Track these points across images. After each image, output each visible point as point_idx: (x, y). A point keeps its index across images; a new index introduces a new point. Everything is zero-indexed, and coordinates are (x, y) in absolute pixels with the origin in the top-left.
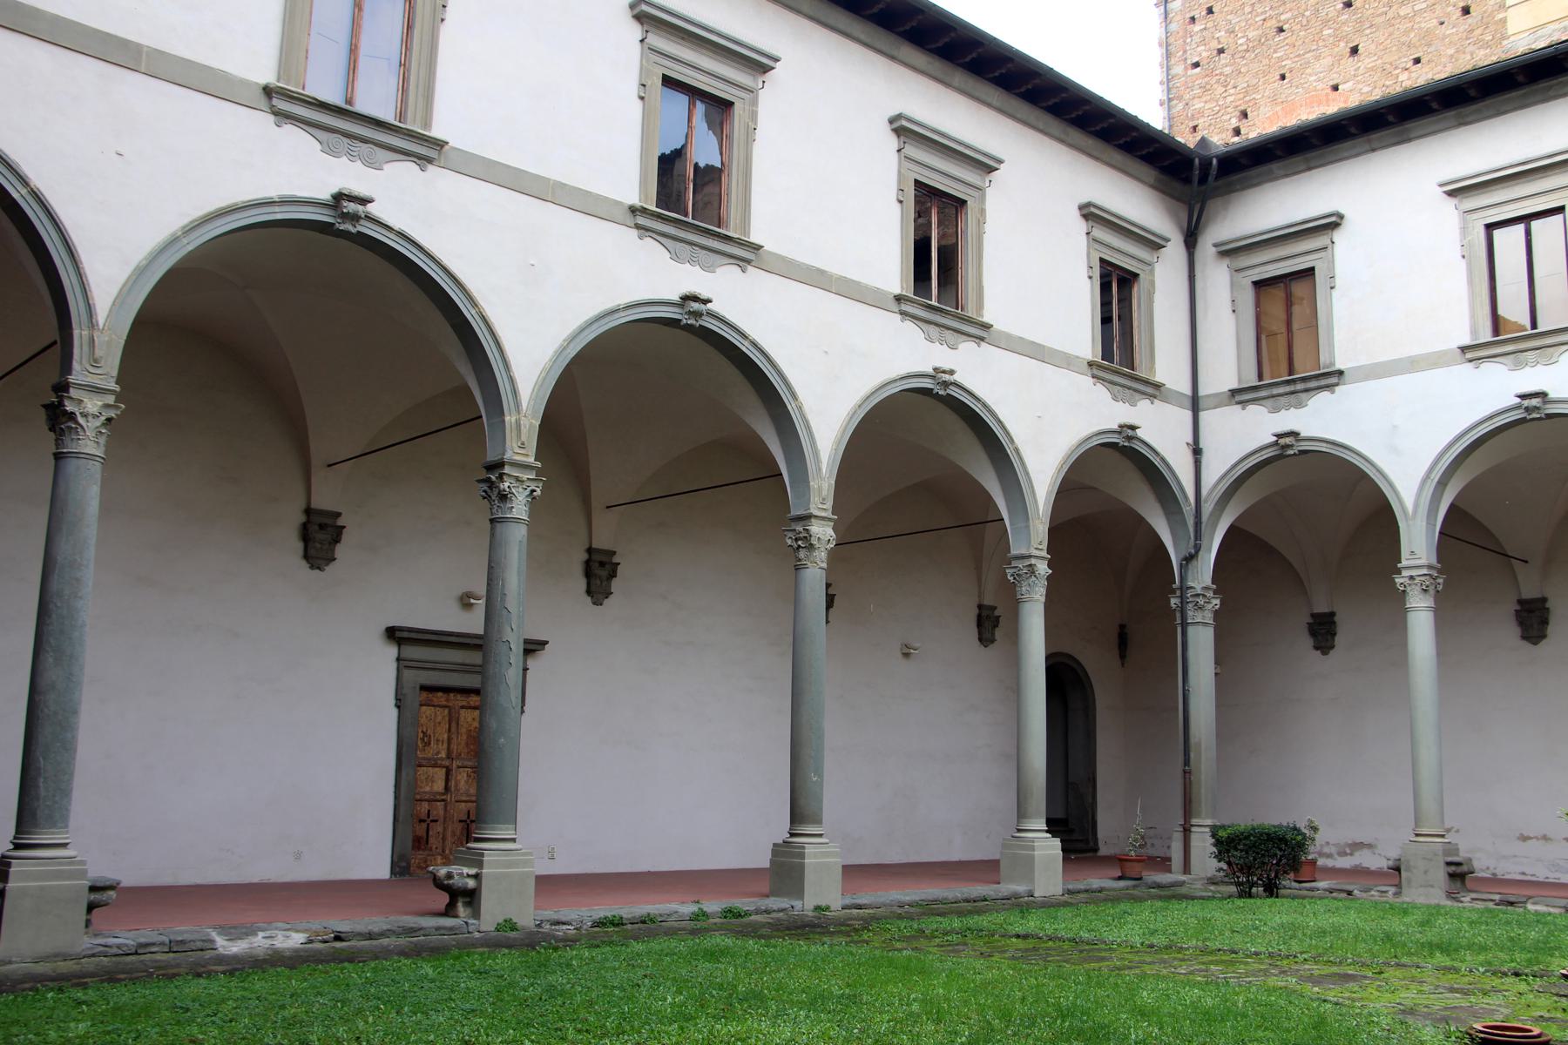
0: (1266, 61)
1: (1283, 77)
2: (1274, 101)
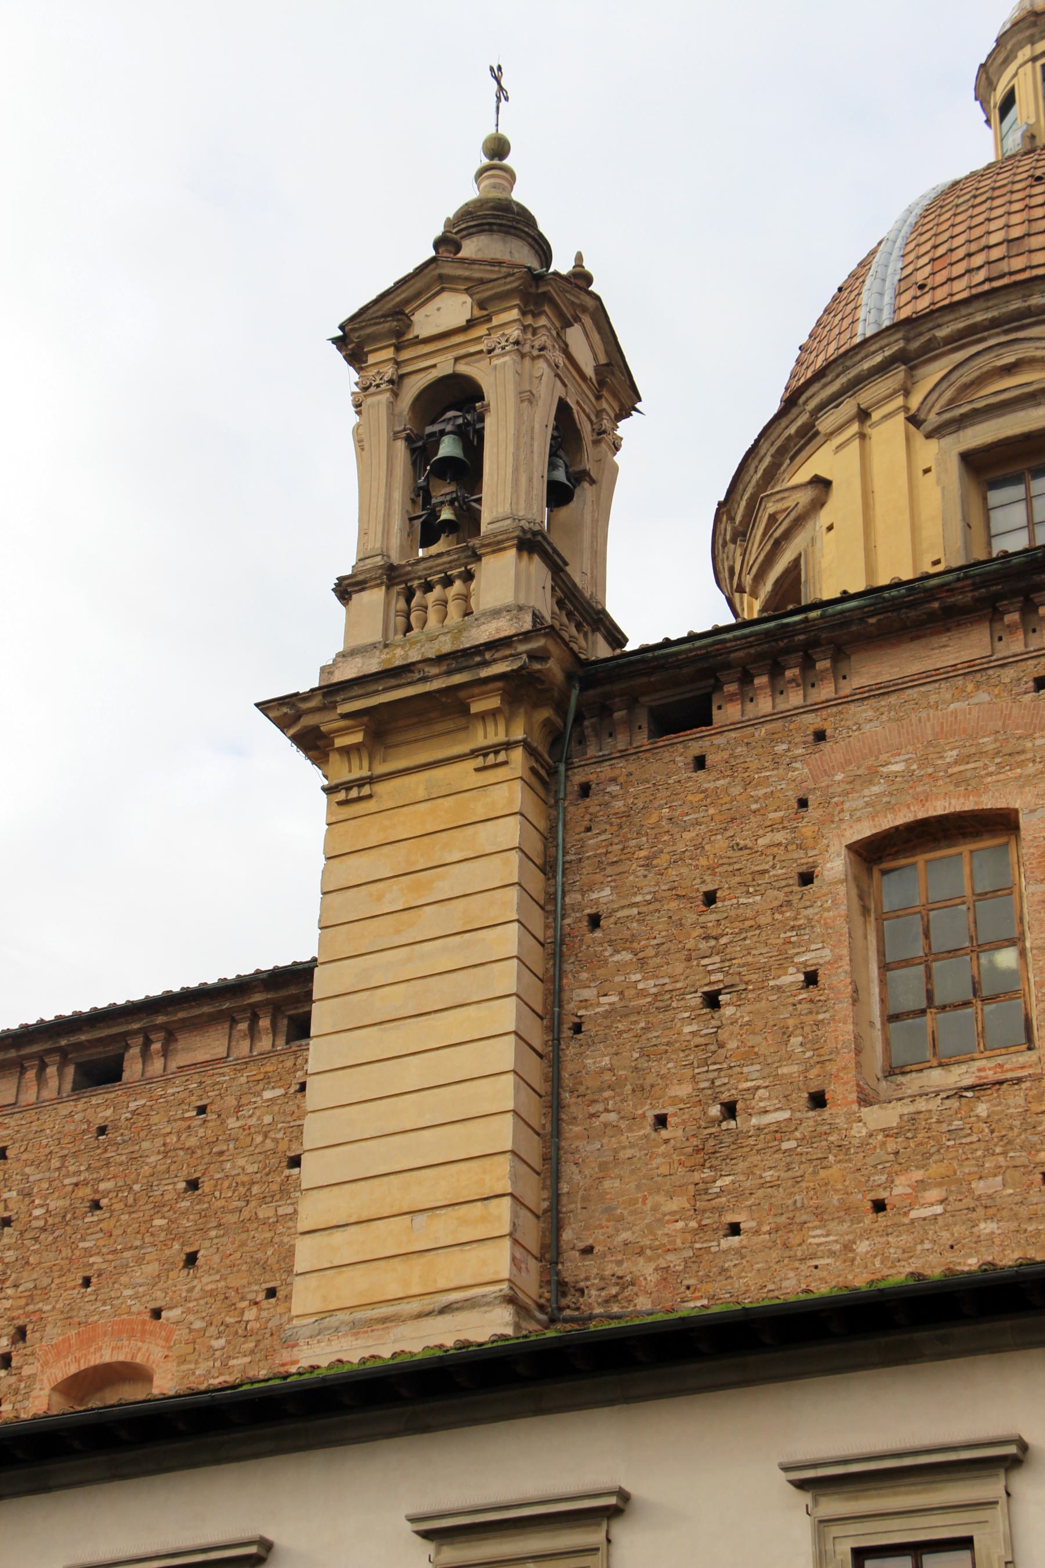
0: (66, 1252)
1: (87, 1282)
2: (67, 1317)
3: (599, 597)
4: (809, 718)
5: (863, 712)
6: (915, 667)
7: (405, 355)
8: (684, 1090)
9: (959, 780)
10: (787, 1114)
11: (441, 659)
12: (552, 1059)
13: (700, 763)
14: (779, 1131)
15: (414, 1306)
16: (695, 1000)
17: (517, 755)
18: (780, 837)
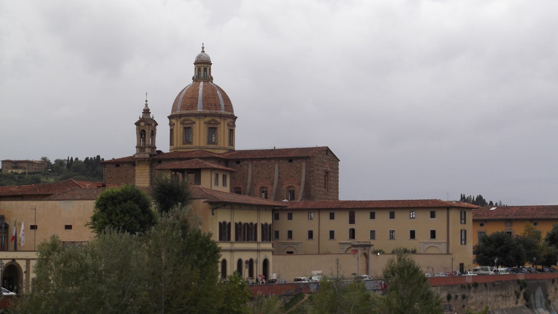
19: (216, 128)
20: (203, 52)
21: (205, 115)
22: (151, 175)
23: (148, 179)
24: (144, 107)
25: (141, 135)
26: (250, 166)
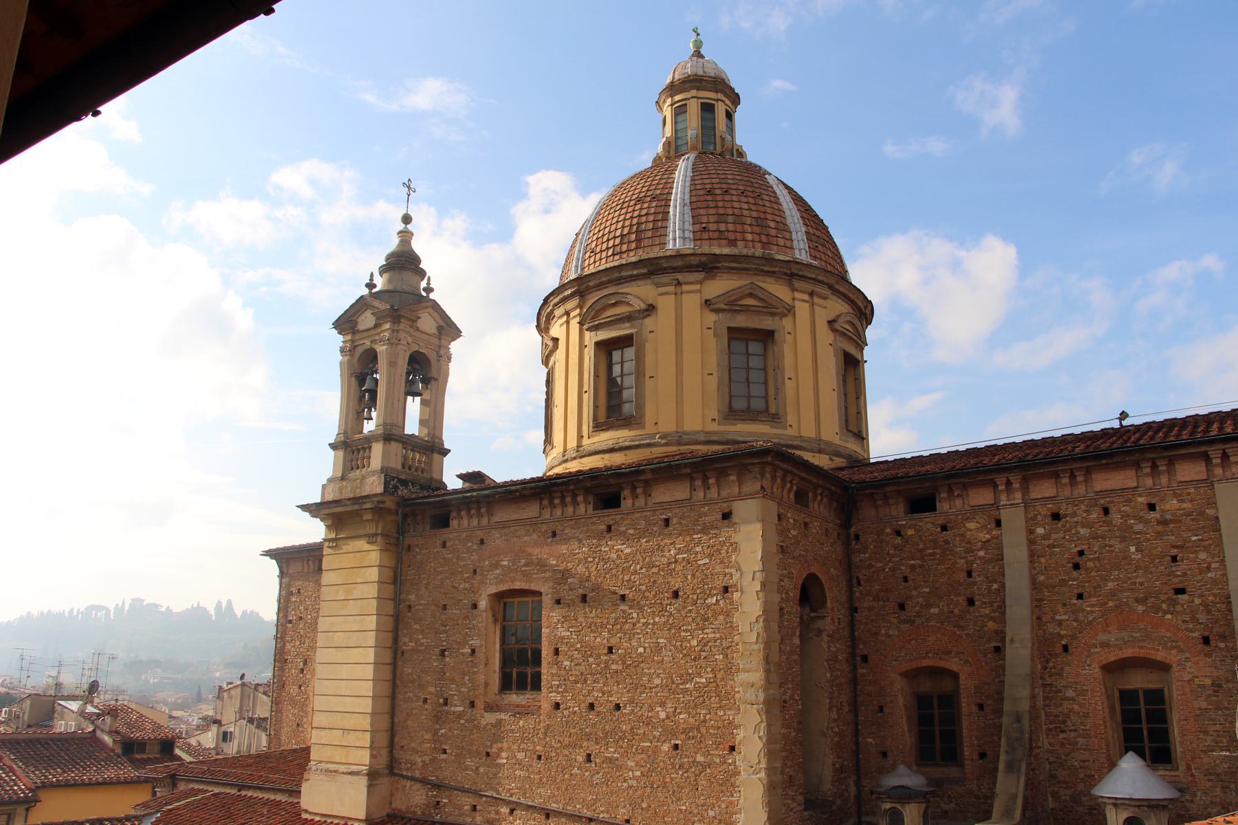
3: (437, 434)
4: (479, 532)
5: (496, 534)
6: (514, 517)
7: (357, 337)
8: (432, 689)
9: (525, 574)
10: (461, 709)
11: (349, 499)
12: (394, 664)
13: (444, 545)
14: (460, 715)
15: (343, 768)
16: (437, 651)
17: (379, 538)
18: (467, 585)
19: (767, 336)
20: (698, 54)
21: (708, 266)
22: (397, 599)
23: (371, 622)
24: (393, 244)
25: (361, 379)
26: (1014, 518)
